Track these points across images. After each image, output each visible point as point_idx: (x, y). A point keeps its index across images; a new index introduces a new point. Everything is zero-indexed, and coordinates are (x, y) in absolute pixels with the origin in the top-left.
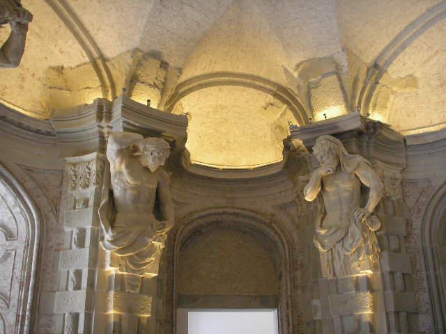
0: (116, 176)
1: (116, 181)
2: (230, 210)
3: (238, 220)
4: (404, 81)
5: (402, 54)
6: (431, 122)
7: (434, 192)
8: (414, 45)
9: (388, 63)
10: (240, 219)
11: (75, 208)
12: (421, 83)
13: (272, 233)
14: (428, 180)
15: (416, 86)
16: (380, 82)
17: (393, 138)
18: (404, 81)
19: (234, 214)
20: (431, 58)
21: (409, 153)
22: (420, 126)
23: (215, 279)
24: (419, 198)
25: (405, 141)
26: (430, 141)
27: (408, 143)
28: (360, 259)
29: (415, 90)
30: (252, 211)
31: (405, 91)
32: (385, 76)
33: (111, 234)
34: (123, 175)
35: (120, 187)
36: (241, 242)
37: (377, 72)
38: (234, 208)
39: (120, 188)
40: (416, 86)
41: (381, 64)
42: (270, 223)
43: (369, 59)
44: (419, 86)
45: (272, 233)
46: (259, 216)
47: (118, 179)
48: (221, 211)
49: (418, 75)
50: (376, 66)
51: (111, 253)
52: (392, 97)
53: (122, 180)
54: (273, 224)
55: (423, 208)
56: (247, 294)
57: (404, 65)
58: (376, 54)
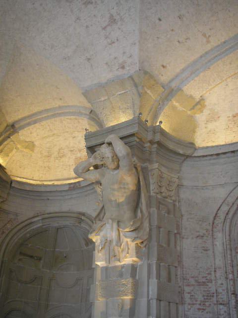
4: (27, 144)
5: (33, 126)
6: (33, 178)
7: (17, 224)
8: (43, 124)
9: (22, 127)
12: (37, 150)
14: (16, 215)
15: (33, 150)
16: (11, 137)
17: (4, 178)
18: (27, 144)
20: (49, 136)
21: (11, 192)
22: (25, 177)
24: (6, 225)
25: (11, 183)
26: (28, 189)
27: (13, 185)
29: (31, 152)
31: (24, 150)
32: (16, 134)
37: (12, 130)
40: (33, 150)
41: (17, 126)
43: (10, 120)
44: (35, 151)
49: (36, 143)
50: (13, 126)
52: (15, 150)
55: (7, 232)
57: (31, 133)
58: (16, 118)
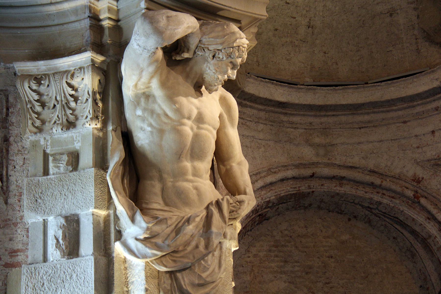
0: (137, 103)
1: (139, 112)
2: (326, 171)
3: (338, 189)
10: (347, 189)
11: (46, 172)
13: (421, 218)
19: (333, 178)
30: (372, 172)
33: (144, 225)
34: (155, 101)
35: (150, 125)
36: (345, 237)
38: (333, 165)
39: (149, 129)
42: (416, 196)
45: (421, 218)
46: (387, 183)
47: (145, 110)
48: (308, 172)
51: (147, 264)
53: (152, 112)
54: (423, 201)
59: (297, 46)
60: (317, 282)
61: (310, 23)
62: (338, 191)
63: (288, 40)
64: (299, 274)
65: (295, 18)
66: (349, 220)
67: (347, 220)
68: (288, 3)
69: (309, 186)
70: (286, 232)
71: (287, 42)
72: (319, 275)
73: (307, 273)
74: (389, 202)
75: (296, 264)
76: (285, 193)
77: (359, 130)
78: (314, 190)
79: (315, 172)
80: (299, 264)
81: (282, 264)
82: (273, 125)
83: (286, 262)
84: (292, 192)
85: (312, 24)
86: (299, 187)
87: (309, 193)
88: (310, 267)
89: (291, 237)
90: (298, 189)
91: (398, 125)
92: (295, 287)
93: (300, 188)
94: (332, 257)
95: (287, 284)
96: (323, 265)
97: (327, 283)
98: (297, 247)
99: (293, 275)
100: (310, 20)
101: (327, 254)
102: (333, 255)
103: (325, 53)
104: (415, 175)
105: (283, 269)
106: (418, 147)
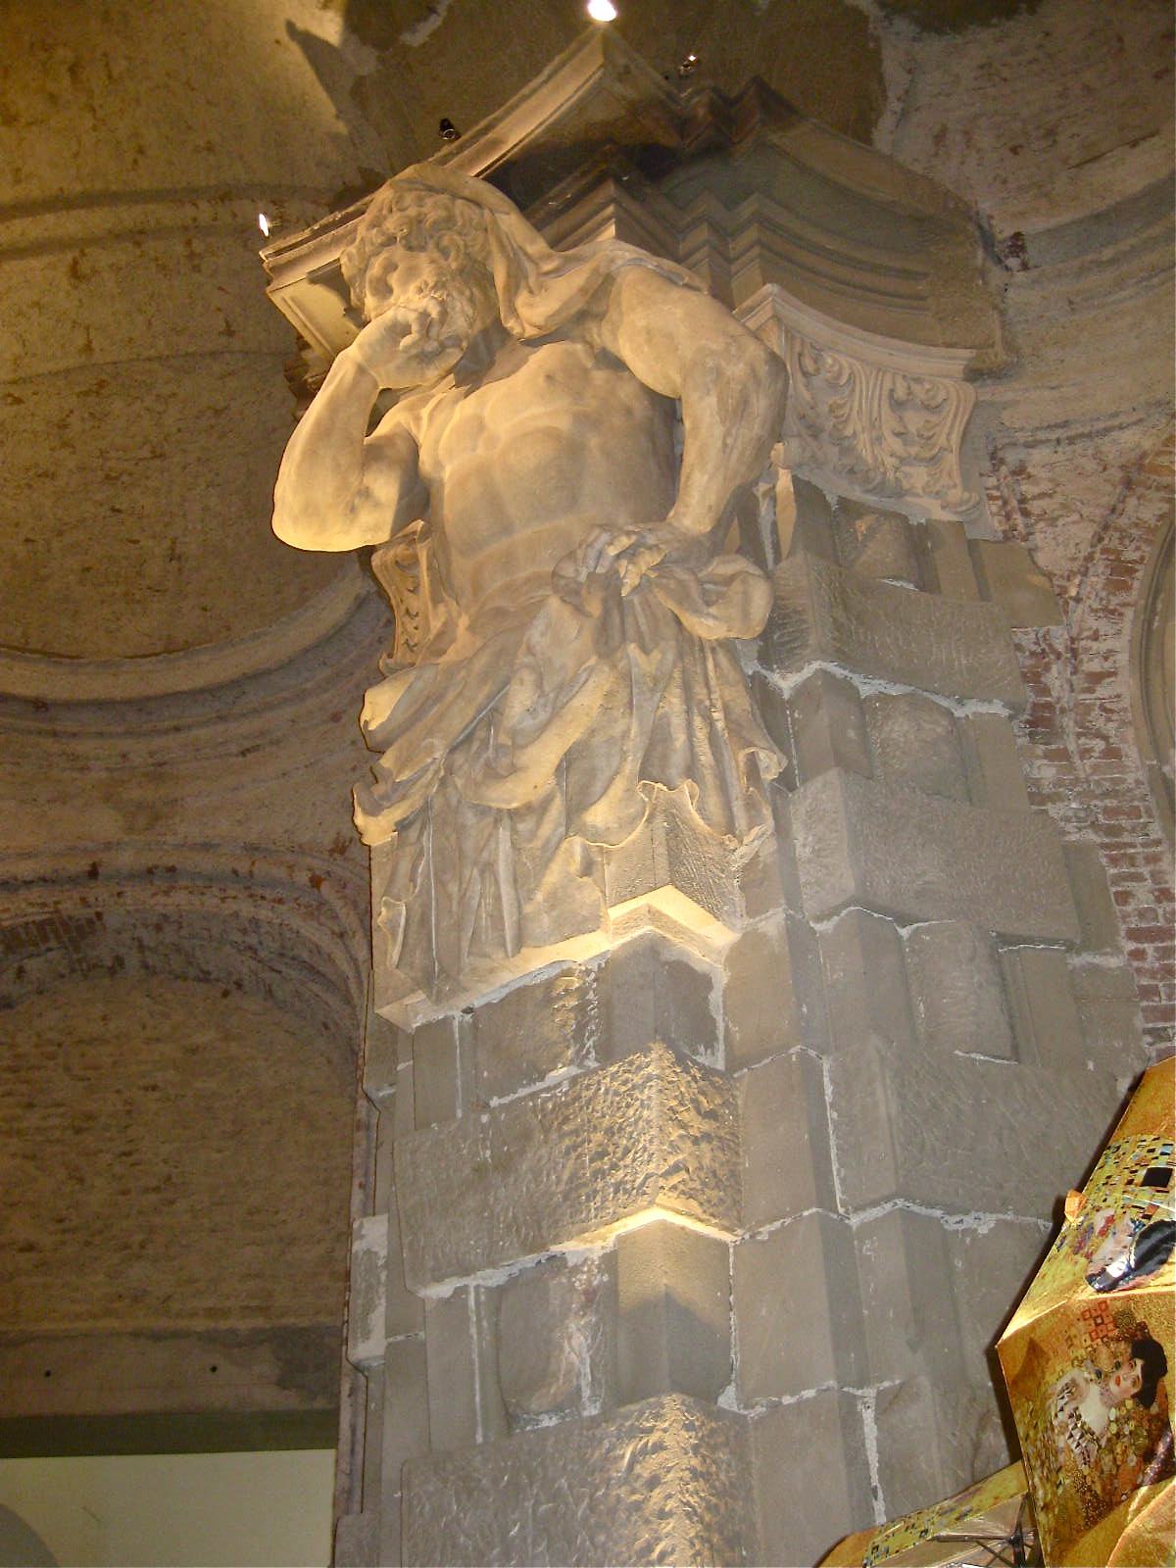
23: (30, 1247)
28: (599, 815)
56: (201, 1324)
59: (139, 602)
60: (101, 1151)
61: (173, 550)
62: (159, 908)
63: (117, 590)
64: (58, 1134)
65: (136, 542)
66: (225, 994)
67: (219, 995)
68: (119, 511)
69: (83, 899)
70: (51, 1035)
71: (114, 594)
72: (108, 1134)
73: (78, 1131)
74: (270, 914)
75: (51, 1111)
76: (12, 918)
77: (241, 759)
78: (99, 909)
79: (96, 860)
80: (61, 1110)
81: (19, 1111)
82: (18, 764)
83: (30, 1106)
84: (38, 918)
85: (177, 551)
86: (57, 903)
87: (90, 922)
88: (90, 1117)
89: (59, 1045)
90: (51, 910)
91: (322, 728)
92: (38, 1168)
93: (60, 906)
94: (154, 1088)
95: (18, 1161)
96: (128, 1107)
97: (124, 1154)
98: (67, 1069)
99: (39, 1138)
100: (174, 543)
101: (143, 1082)
102: (160, 1084)
103: (205, 609)
104: (337, 838)
105: (15, 1125)
106: (354, 769)
